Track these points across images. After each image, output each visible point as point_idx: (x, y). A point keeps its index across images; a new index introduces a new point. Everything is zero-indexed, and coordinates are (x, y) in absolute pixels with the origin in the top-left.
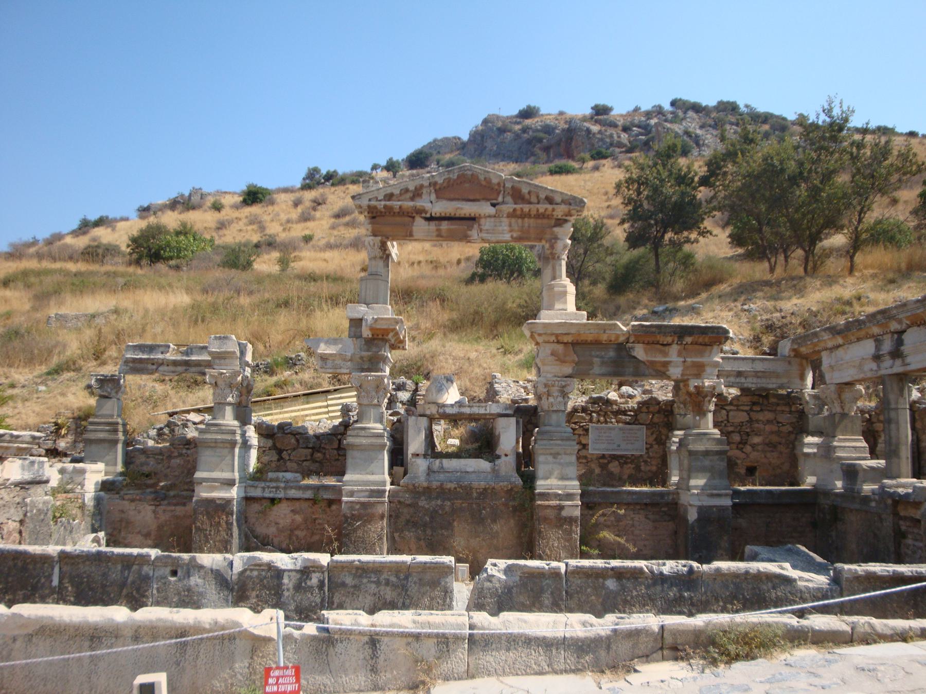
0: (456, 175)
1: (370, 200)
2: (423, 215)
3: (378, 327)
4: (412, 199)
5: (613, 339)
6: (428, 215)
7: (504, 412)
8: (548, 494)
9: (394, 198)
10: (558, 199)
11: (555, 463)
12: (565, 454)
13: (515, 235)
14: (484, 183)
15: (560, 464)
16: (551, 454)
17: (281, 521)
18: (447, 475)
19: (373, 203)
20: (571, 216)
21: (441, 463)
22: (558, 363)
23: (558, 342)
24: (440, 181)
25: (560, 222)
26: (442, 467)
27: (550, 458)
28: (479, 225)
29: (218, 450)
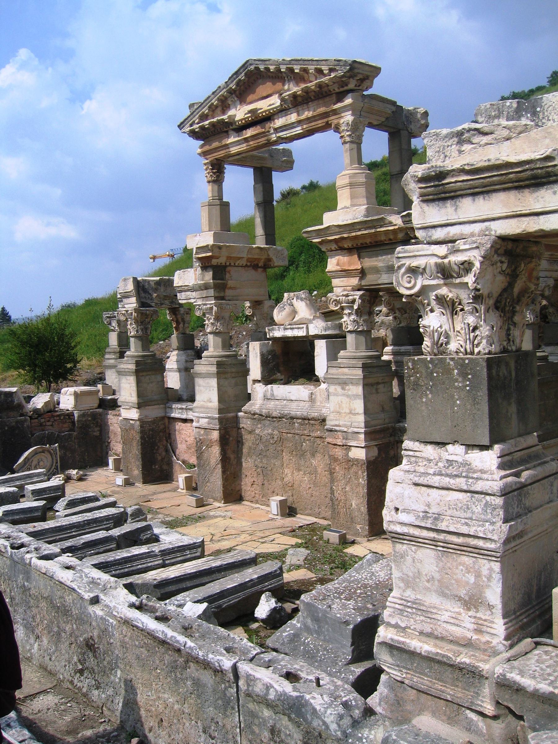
0: (243, 74)
1: (191, 125)
2: (231, 127)
3: (200, 256)
4: (224, 113)
5: (392, 237)
6: (234, 127)
7: (324, 333)
8: (336, 431)
9: (209, 117)
10: (325, 69)
11: (343, 395)
12: (352, 383)
13: (305, 126)
14: (269, 74)
15: (348, 396)
16: (339, 384)
17: (188, 439)
18: (277, 403)
19: (195, 126)
20: (347, 85)
21: (272, 390)
22: (343, 273)
23: (342, 249)
24: (233, 86)
25: (340, 97)
26: (273, 395)
27: (339, 388)
28: (274, 124)
29: (128, 378)
